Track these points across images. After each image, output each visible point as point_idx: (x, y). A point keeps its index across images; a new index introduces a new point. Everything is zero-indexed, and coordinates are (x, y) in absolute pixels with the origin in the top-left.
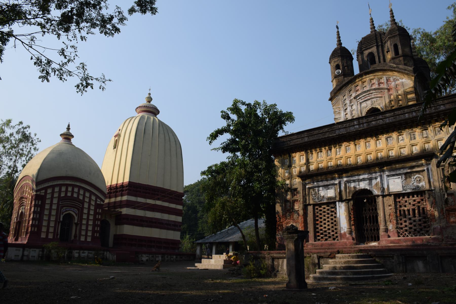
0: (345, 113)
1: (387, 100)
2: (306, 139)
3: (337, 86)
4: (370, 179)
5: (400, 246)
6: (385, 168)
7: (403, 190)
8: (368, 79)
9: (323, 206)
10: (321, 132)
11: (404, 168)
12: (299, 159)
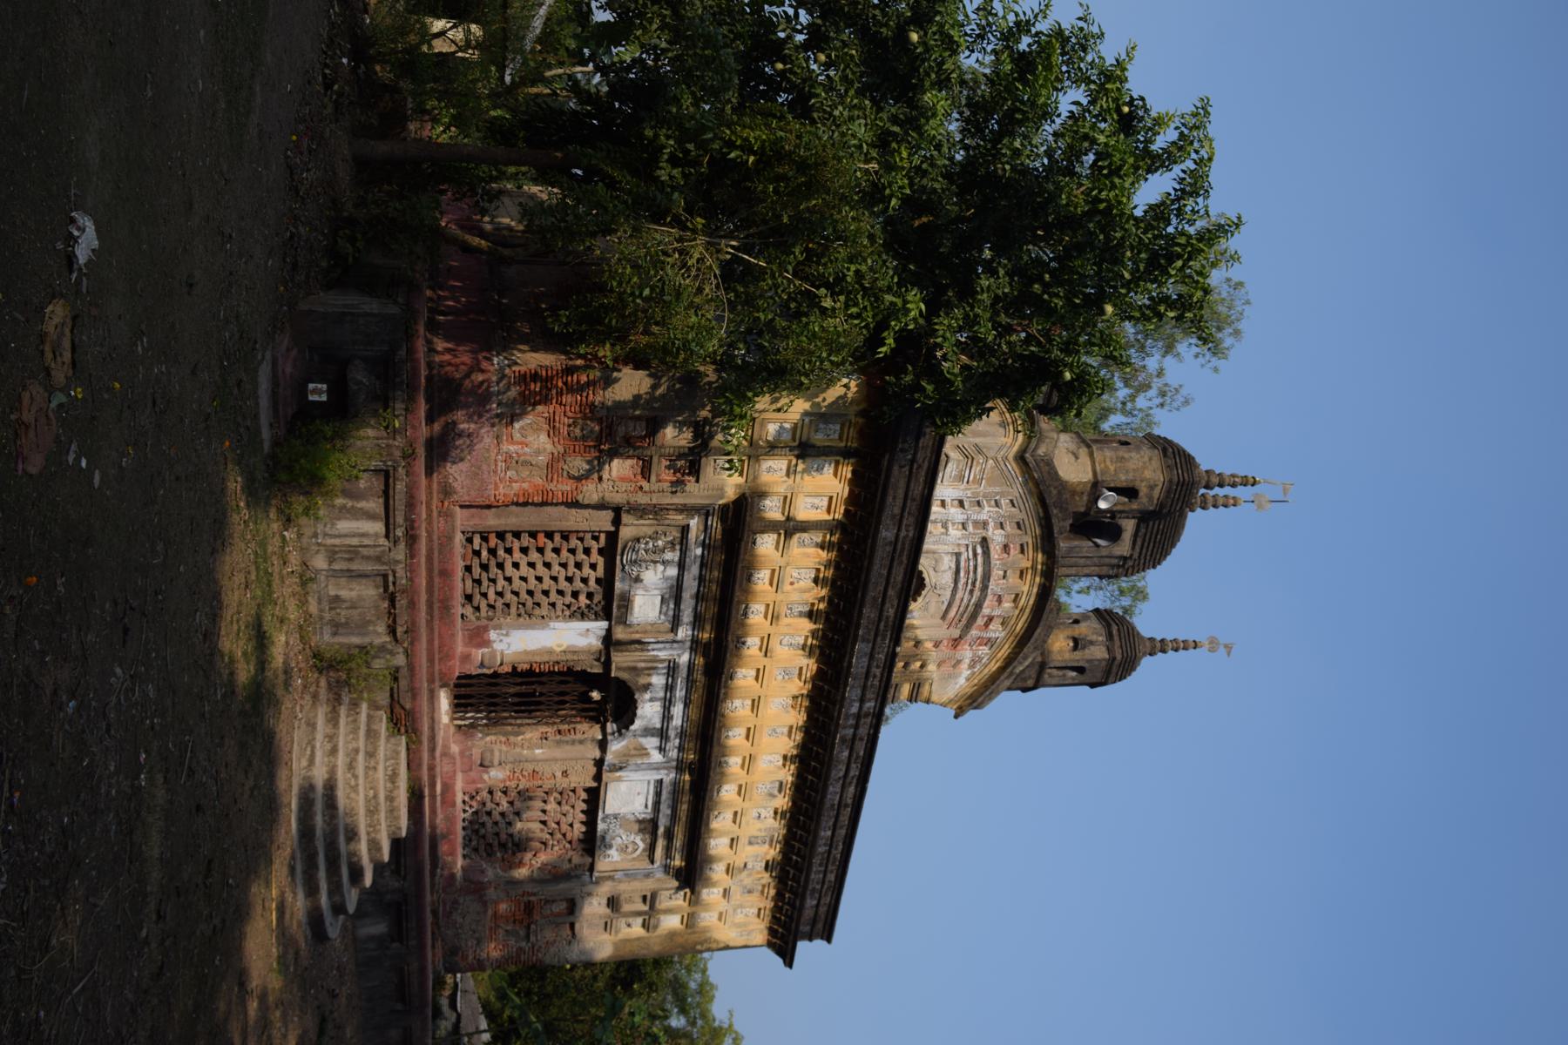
0: (948, 501)
1: (921, 634)
2: (887, 533)
3: (1063, 486)
4: (662, 734)
5: (433, 811)
6: (687, 777)
7: (607, 816)
8: (1025, 589)
9: (601, 561)
10: (891, 592)
11: (674, 817)
12: (819, 492)
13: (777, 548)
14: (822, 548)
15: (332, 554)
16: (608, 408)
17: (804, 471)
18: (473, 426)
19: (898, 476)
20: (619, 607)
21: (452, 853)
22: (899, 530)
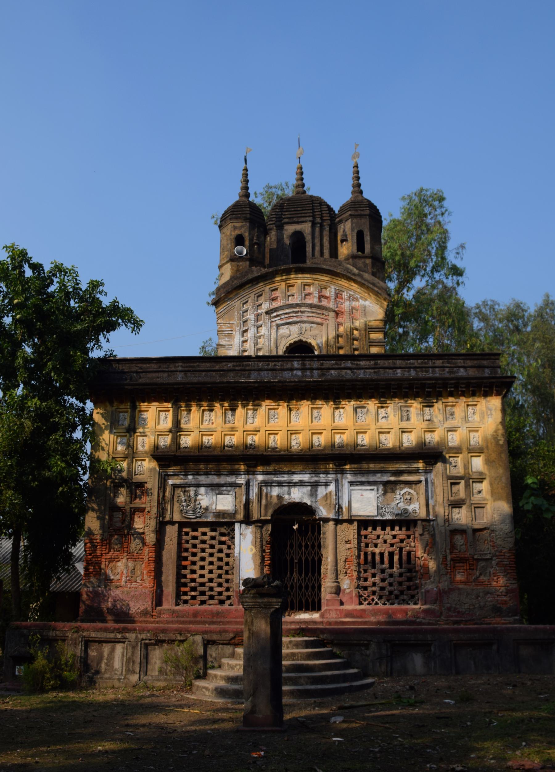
0: (242, 339)
1: (332, 334)
2: (180, 377)
3: (232, 278)
4: (315, 485)
5: (365, 623)
6: (347, 467)
7: (379, 514)
8: (299, 281)
9: (200, 530)
10: (217, 367)
11: (383, 472)
12: (156, 419)
13: (189, 435)
14: (190, 410)
15: (131, 671)
16: (104, 532)
17: (144, 428)
18: (110, 600)
19: (145, 379)
20: (224, 518)
21: (406, 612)
22: (177, 371)
